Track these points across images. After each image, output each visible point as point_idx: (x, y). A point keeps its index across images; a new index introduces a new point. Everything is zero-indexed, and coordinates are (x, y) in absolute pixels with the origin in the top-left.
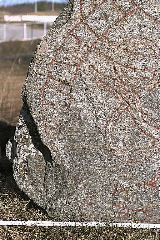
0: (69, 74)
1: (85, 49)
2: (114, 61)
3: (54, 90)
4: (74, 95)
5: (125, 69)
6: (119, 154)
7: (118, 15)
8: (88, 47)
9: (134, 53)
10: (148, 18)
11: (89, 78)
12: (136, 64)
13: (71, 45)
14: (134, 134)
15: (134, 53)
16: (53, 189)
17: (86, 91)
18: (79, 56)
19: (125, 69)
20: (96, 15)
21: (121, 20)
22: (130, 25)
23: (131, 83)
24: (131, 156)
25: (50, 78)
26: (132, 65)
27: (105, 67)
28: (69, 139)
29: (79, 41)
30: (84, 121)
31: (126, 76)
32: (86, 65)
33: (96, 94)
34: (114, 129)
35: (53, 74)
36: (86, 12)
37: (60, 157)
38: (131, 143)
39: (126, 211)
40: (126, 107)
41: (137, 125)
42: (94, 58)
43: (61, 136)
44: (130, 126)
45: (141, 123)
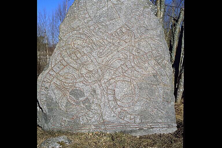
0: (47, 85)
1: (53, 77)
2: (61, 81)
3: (43, 90)
4: (49, 92)
5: (64, 83)
8: (53, 77)
9: (67, 78)
10: (71, 67)
11: (53, 86)
12: (68, 82)
13: (48, 76)
15: (67, 78)
16: (44, 121)
18: (50, 79)
19: (64, 83)
20: (55, 67)
22: (66, 70)
24: (66, 110)
25: (42, 86)
27: (58, 83)
28: (48, 105)
30: (52, 100)
31: (65, 85)
32: (53, 82)
33: (55, 91)
34: (61, 102)
35: (43, 85)
37: (45, 111)
38: (66, 106)
39: (65, 127)
40: (65, 95)
42: (55, 79)
43: (46, 104)
44: (66, 101)
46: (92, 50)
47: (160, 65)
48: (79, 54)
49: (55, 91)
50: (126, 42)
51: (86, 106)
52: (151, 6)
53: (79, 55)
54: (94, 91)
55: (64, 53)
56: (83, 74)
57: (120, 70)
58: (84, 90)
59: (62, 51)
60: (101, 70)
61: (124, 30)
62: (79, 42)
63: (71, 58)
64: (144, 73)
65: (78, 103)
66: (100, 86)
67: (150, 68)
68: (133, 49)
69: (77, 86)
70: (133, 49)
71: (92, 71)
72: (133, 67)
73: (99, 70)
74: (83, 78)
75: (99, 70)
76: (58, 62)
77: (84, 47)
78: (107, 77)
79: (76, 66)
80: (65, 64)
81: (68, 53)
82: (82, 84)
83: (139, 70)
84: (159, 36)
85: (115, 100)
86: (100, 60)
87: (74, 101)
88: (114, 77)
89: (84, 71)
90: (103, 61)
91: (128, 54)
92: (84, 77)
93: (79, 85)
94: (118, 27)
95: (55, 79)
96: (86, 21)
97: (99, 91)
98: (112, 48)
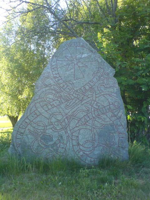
0: (23, 131)
2: (34, 128)
4: (24, 136)
6: (34, 151)
7: (36, 116)
10: (43, 117)
11: (27, 131)
12: (39, 128)
14: (38, 146)
17: (27, 135)
21: (36, 117)
22: (38, 119)
23: (38, 133)
26: (39, 129)
27: (32, 129)
29: (26, 122)
30: (26, 143)
32: (27, 128)
33: (29, 136)
36: (28, 115)
41: (39, 144)
45: (40, 144)
46: (61, 103)
47: (116, 116)
48: (50, 106)
49: (29, 136)
50: (89, 98)
51: (54, 149)
52: (110, 69)
53: (50, 107)
54: (62, 137)
55: (38, 105)
56: (52, 122)
57: (83, 120)
58: (52, 136)
59: (36, 103)
60: (68, 120)
61: (87, 88)
62: (51, 96)
63: (44, 109)
64: (103, 123)
65: (47, 147)
66: (66, 132)
67: (108, 119)
68: (94, 103)
69: (47, 131)
70: (94, 103)
71: (60, 120)
72: (94, 118)
73: (66, 120)
74: (52, 126)
75: (66, 120)
76: (33, 112)
77: (54, 100)
78: (72, 125)
79: (47, 116)
80: (38, 114)
81: (41, 105)
82: (51, 131)
83: (99, 120)
84: (116, 93)
85: (78, 144)
86: (67, 111)
87: (44, 144)
88: (77, 125)
89: (53, 120)
90: (69, 112)
91: (90, 107)
92: (53, 124)
93: (49, 132)
94: (82, 85)
95: (29, 126)
96: (56, 79)
97: (65, 137)
98: (77, 102)
